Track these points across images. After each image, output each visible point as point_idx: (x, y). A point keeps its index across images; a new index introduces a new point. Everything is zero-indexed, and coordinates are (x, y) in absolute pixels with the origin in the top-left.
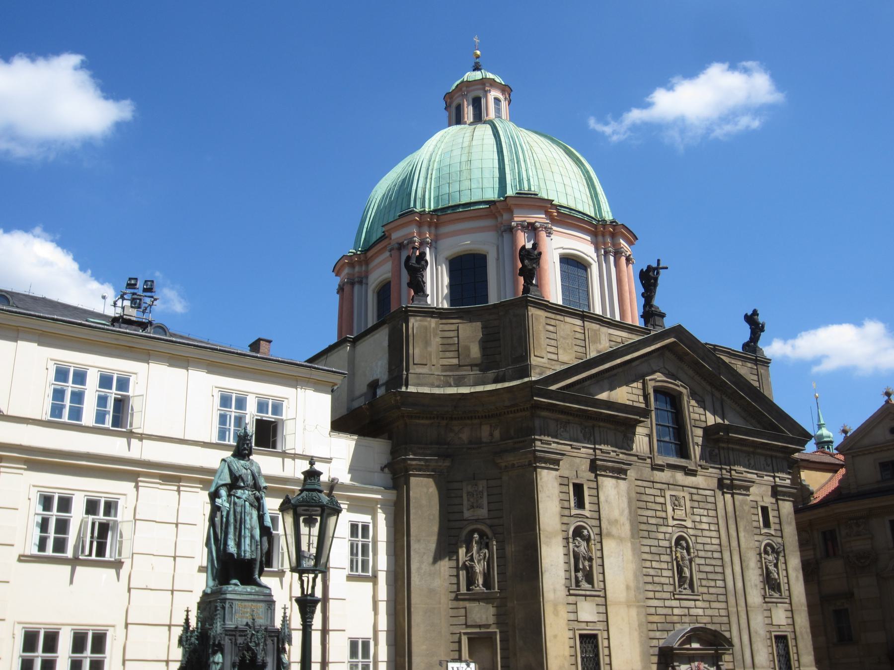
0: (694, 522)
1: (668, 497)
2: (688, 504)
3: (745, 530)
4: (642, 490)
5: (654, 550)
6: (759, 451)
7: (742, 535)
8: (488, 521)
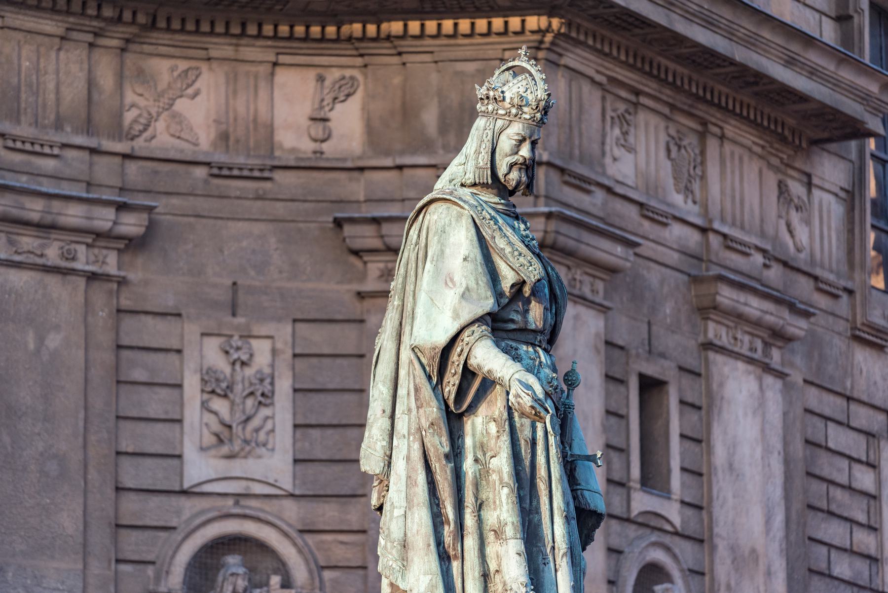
8: (291, 511)
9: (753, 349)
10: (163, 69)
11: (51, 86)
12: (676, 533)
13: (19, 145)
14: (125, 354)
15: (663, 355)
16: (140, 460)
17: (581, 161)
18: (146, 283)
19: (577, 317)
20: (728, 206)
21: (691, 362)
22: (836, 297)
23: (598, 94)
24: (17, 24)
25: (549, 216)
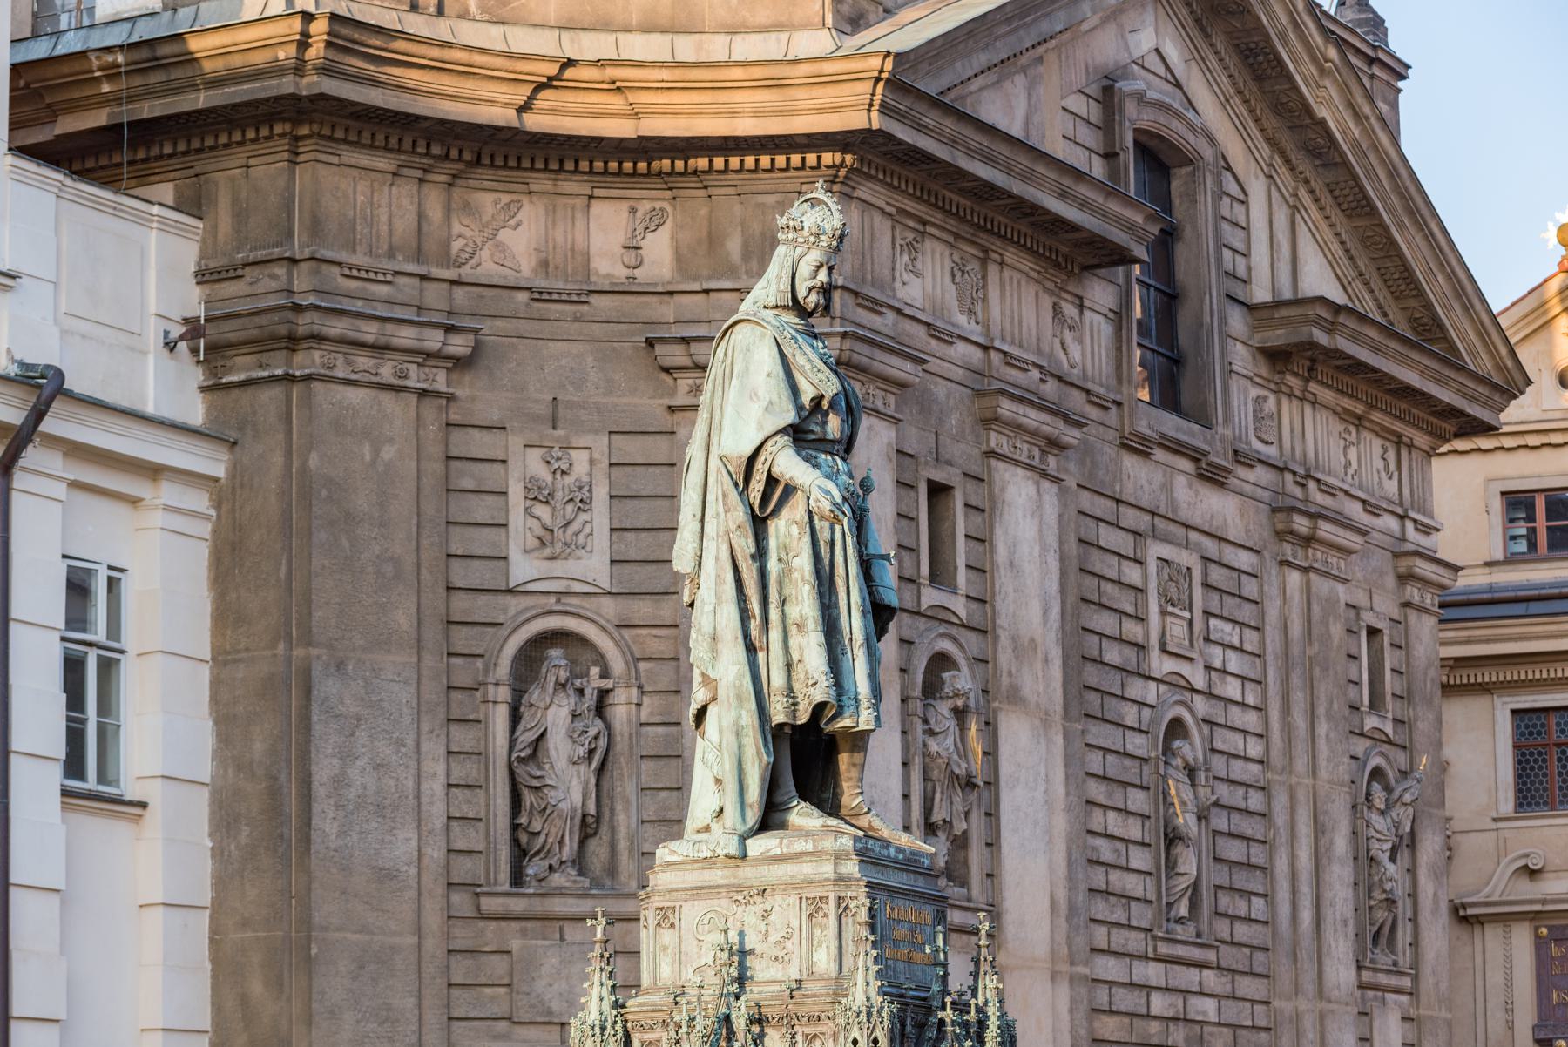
0: (1208, 668)
1: (1152, 566)
2: (1198, 592)
3: (1329, 717)
4: (1089, 529)
5: (1114, 766)
6: (1377, 416)
7: (1322, 728)
8: (609, 608)
9: (1031, 457)
10: (488, 202)
11: (384, 218)
12: (963, 625)
13: (355, 273)
14: (454, 464)
15: (949, 463)
16: (469, 561)
17: (873, 285)
18: (473, 399)
19: (870, 428)
20: (1008, 326)
21: (975, 469)
22: (1106, 408)
23: (889, 224)
24: (353, 161)
25: (844, 335)
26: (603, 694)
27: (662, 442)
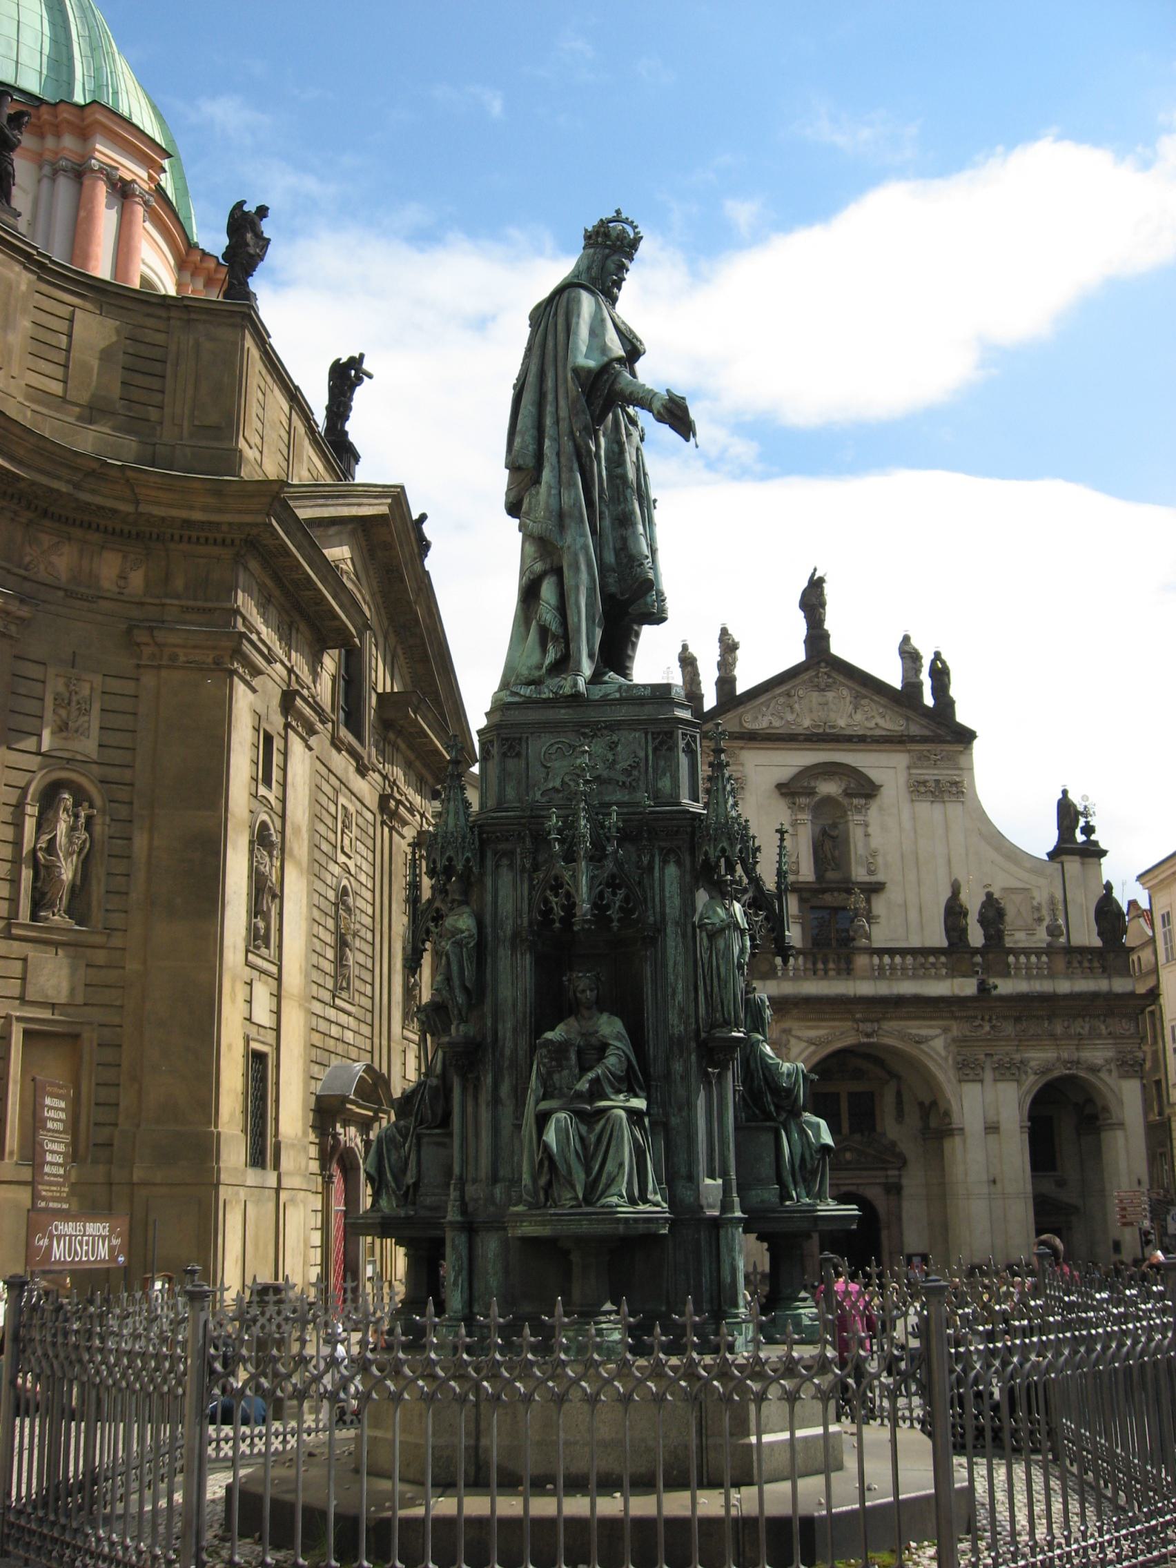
1: (340, 807)
10: (46, 540)
26: (89, 818)
27: (132, 684)
